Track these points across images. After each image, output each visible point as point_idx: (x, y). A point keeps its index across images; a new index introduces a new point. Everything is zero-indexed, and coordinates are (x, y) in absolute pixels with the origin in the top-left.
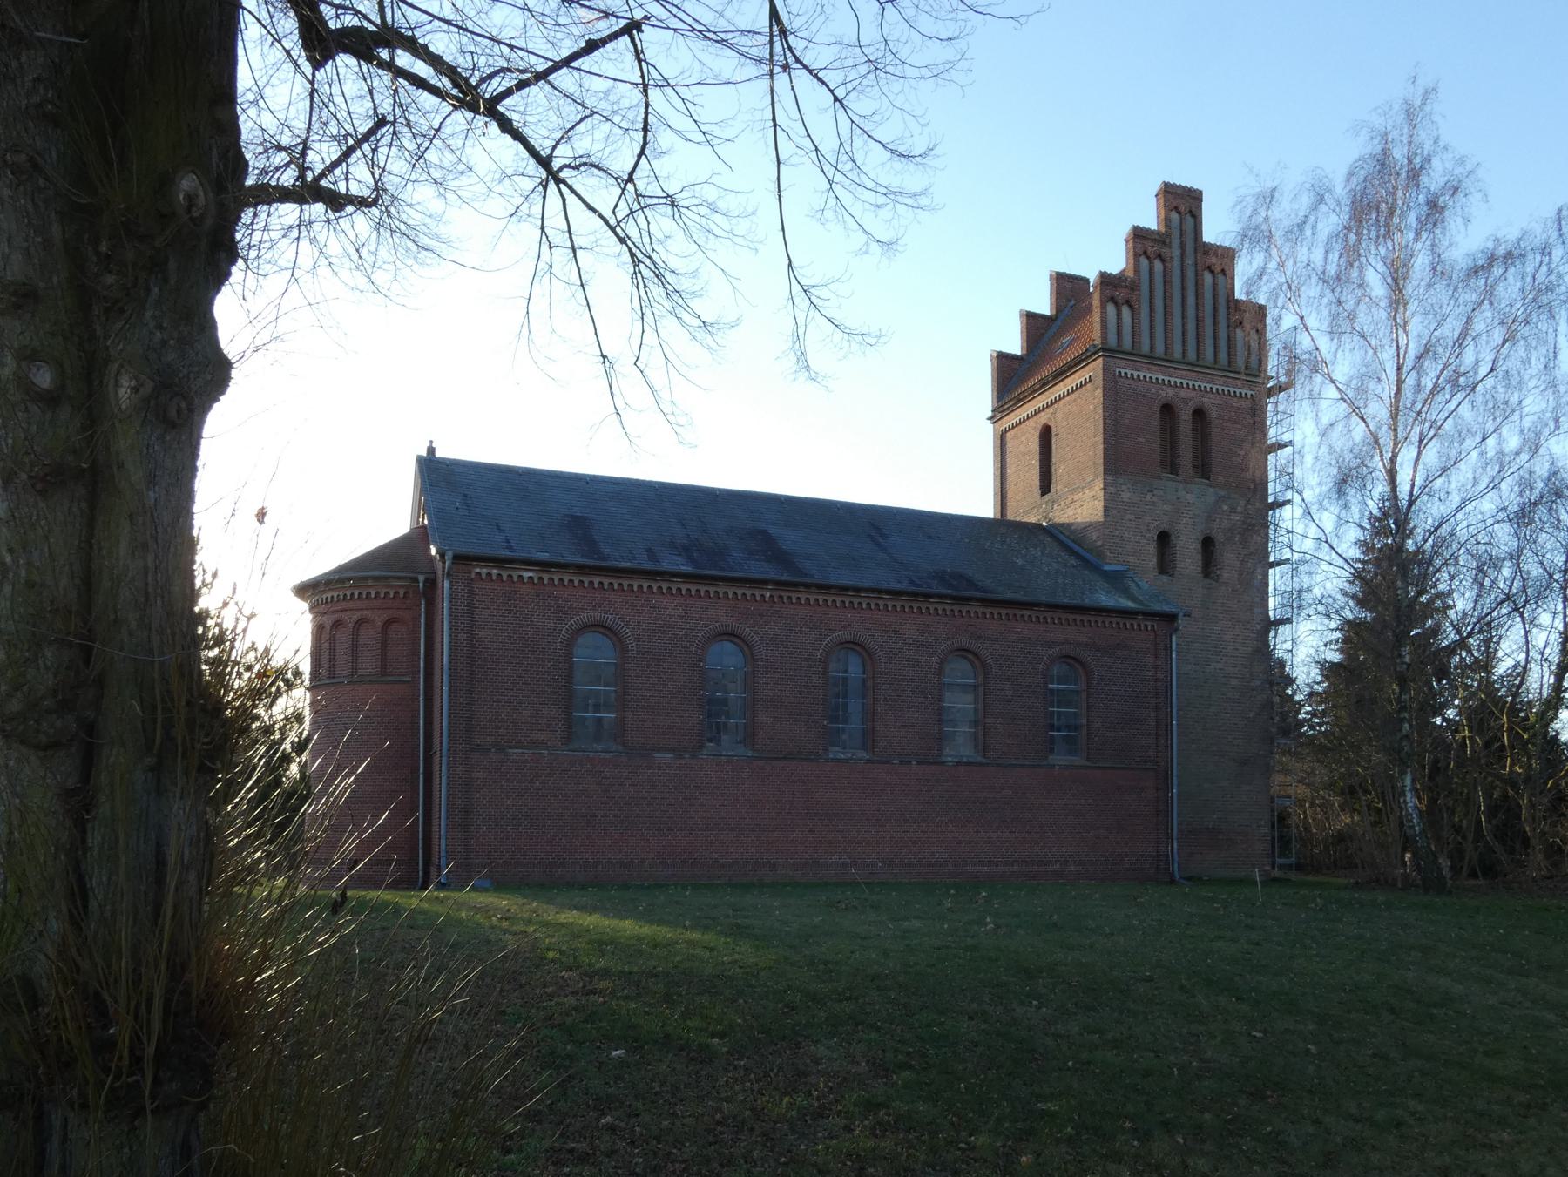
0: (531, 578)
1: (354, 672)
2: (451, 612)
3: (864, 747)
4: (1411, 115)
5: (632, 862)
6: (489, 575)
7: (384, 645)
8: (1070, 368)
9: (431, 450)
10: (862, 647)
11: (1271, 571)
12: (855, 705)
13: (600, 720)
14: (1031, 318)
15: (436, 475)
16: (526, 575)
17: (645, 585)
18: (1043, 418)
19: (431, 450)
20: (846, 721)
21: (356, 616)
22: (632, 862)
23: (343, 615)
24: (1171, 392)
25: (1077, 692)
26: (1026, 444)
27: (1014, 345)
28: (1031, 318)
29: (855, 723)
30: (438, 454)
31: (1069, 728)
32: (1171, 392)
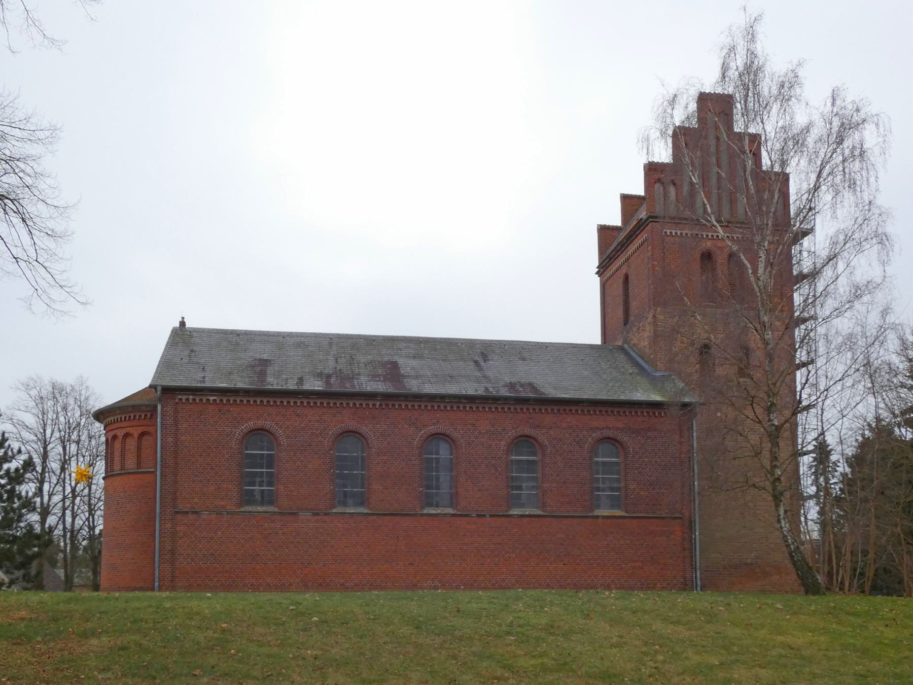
0: (215, 400)
1: (122, 468)
2: (162, 424)
3: (451, 505)
4: (800, 64)
5: (284, 585)
6: (187, 399)
7: (139, 448)
8: (635, 232)
9: (182, 324)
10: (448, 436)
11: (798, 373)
12: (444, 478)
13: (262, 491)
14: (626, 199)
15: (182, 336)
16: (212, 398)
17: (364, 403)
18: (624, 271)
19: (182, 324)
20: (438, 488)
21: (124, 431)
22: (284, 585)
23: (130, 430)
24: (709, 244)
25: (617, 464)
26: (617, 287)
27: (615, 219)
28: (626, 199)
29: (445, 489)
30: (188, 325)
31: (612, 489)
32: (709, 244)
